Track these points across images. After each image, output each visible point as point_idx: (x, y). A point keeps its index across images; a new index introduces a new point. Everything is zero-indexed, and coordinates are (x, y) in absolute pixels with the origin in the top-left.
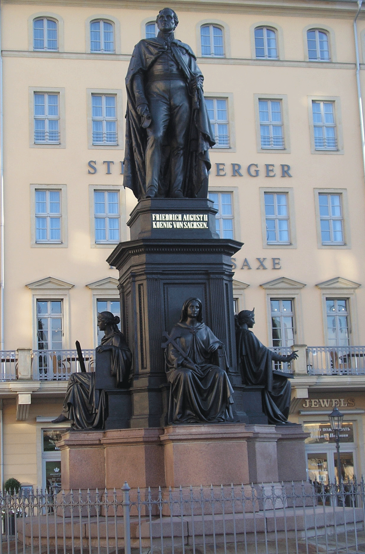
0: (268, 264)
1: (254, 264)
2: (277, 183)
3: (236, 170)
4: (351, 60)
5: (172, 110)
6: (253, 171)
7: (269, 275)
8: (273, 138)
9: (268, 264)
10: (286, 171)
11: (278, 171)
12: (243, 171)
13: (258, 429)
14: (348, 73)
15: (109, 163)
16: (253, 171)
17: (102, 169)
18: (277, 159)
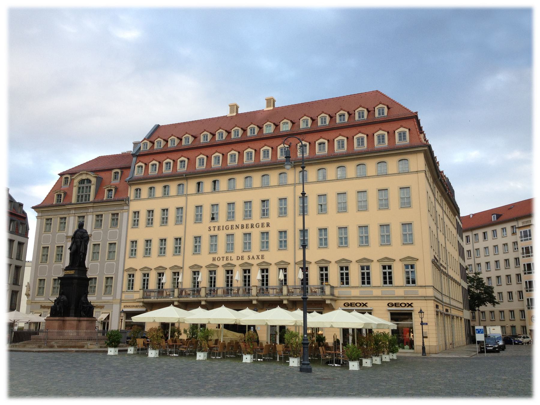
0: (260, 257)
1: (256, 257)
2: (265, 229)
3: (252, 226)
4: (293, 183)
5: (77, 246)
6: (257, 226)
7: (261, 261)
8: (265, 213)
9: (260, 257)
10: (268, 225)
11: (265, 225)
12: (254, 226)
13: (68, 318)
14: (293, 187)
15: (214, 227)
16: (257, 226)
17: (212, 229)
18: (265, 221)
